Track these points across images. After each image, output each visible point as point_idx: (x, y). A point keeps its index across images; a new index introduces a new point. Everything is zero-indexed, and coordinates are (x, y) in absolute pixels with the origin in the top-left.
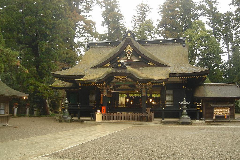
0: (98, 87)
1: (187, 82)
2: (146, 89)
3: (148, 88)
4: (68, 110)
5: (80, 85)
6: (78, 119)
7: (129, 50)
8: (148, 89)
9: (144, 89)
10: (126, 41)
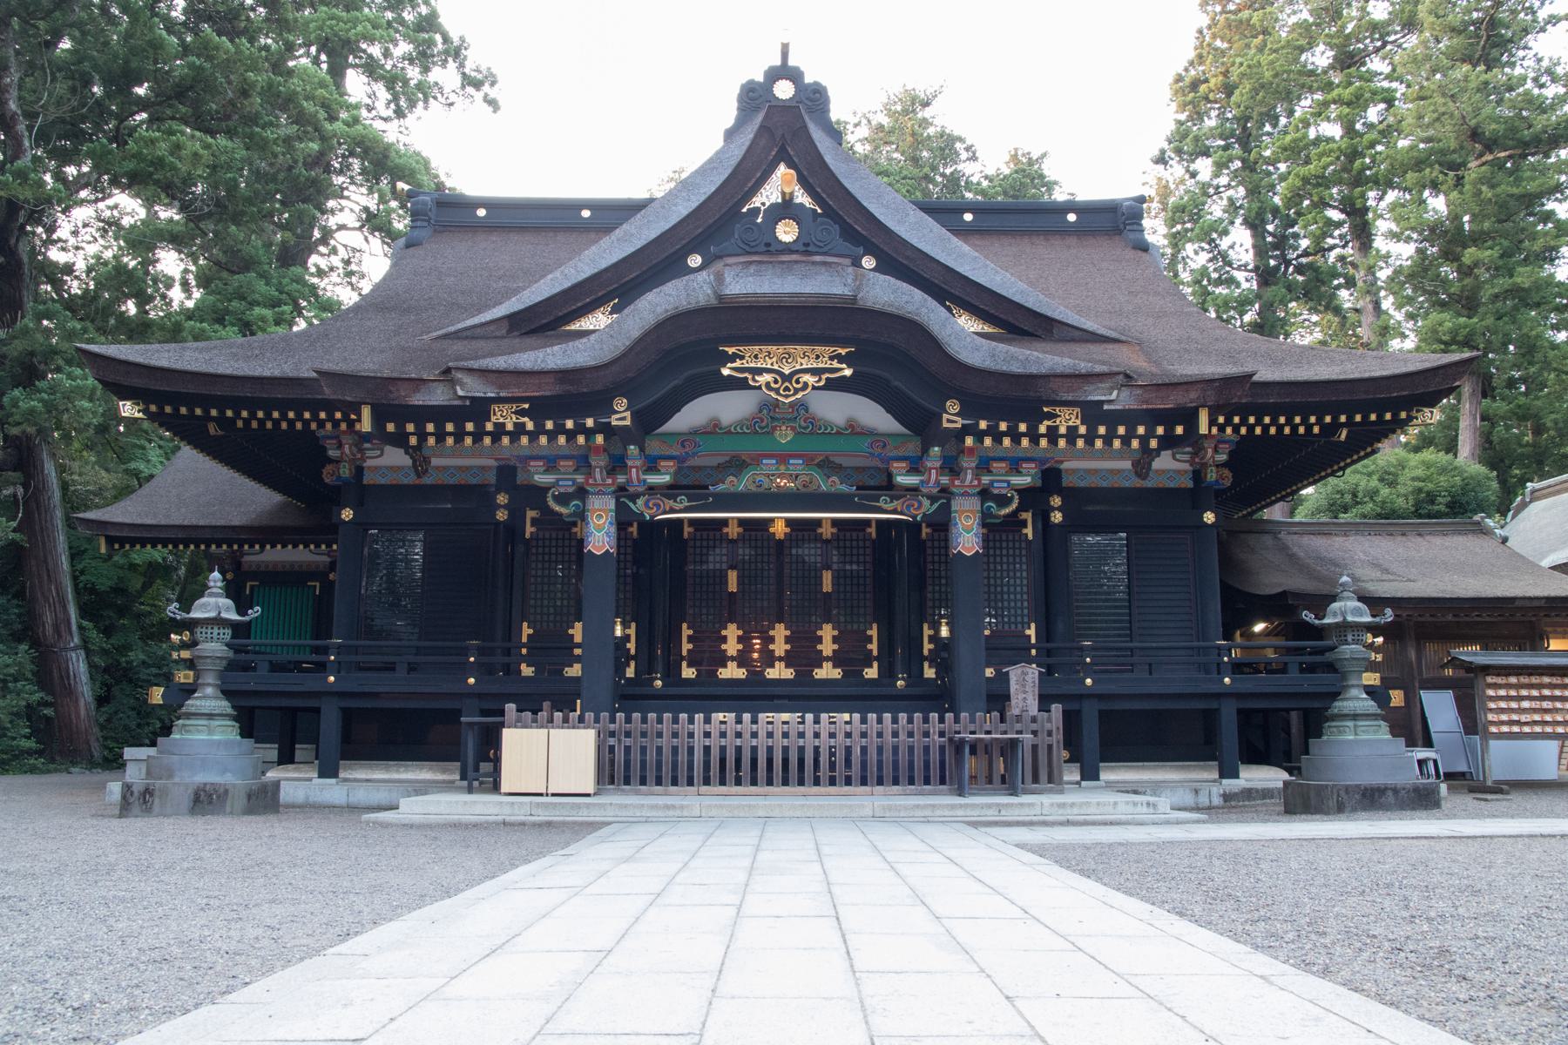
0: (536, 477)
2: (985, 494)
6: (321, 776)
8: (1003, 501)
9: (965, 494)
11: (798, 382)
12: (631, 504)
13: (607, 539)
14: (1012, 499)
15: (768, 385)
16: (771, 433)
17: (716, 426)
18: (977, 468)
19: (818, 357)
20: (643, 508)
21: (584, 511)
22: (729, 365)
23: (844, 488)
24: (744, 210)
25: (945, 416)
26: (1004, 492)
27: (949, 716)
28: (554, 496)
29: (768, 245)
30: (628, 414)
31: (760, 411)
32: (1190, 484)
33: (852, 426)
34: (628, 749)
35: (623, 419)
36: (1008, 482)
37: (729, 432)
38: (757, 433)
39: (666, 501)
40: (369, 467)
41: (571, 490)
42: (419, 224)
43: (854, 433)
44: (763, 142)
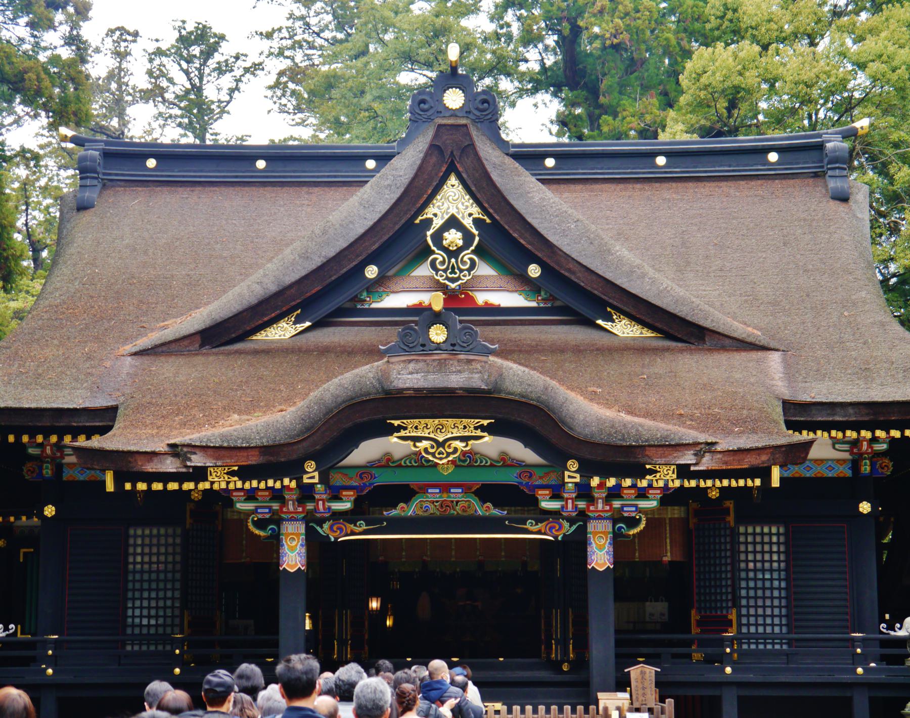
1: (887, 467)
2: (617, 518)
3: (629, 512)
5: (110, 487)
7: (453, 223)
8: (632, 522)
9: (599, 518)
10: (434, 148)
11: (449, 446)
12: (318, 529)
13: (299, 559)
14: (640, 518)
15: (426, 450)
17: (388, 460)
18: (606, 497)
19: (465, 427)
20: (328, 532)
21: (279, 534)
22: (396, 434)
23: (496, 512)
24: (417, 221)
25: (567, 473)
26: (633, 515)
27: (580, 708)
28: (253, 521)
29: (423, 345)
30: (316, 474)
32: (849, 474)
33: (503, 459)
35: (313, 477)
36: (636, 506)
37: (400, 466)
38: (423, 466)
39: (348, 525)
40: (66, 464)
41: (268, 516)
42: (88, 182)
43: (505, 465)
44: (434, 159)
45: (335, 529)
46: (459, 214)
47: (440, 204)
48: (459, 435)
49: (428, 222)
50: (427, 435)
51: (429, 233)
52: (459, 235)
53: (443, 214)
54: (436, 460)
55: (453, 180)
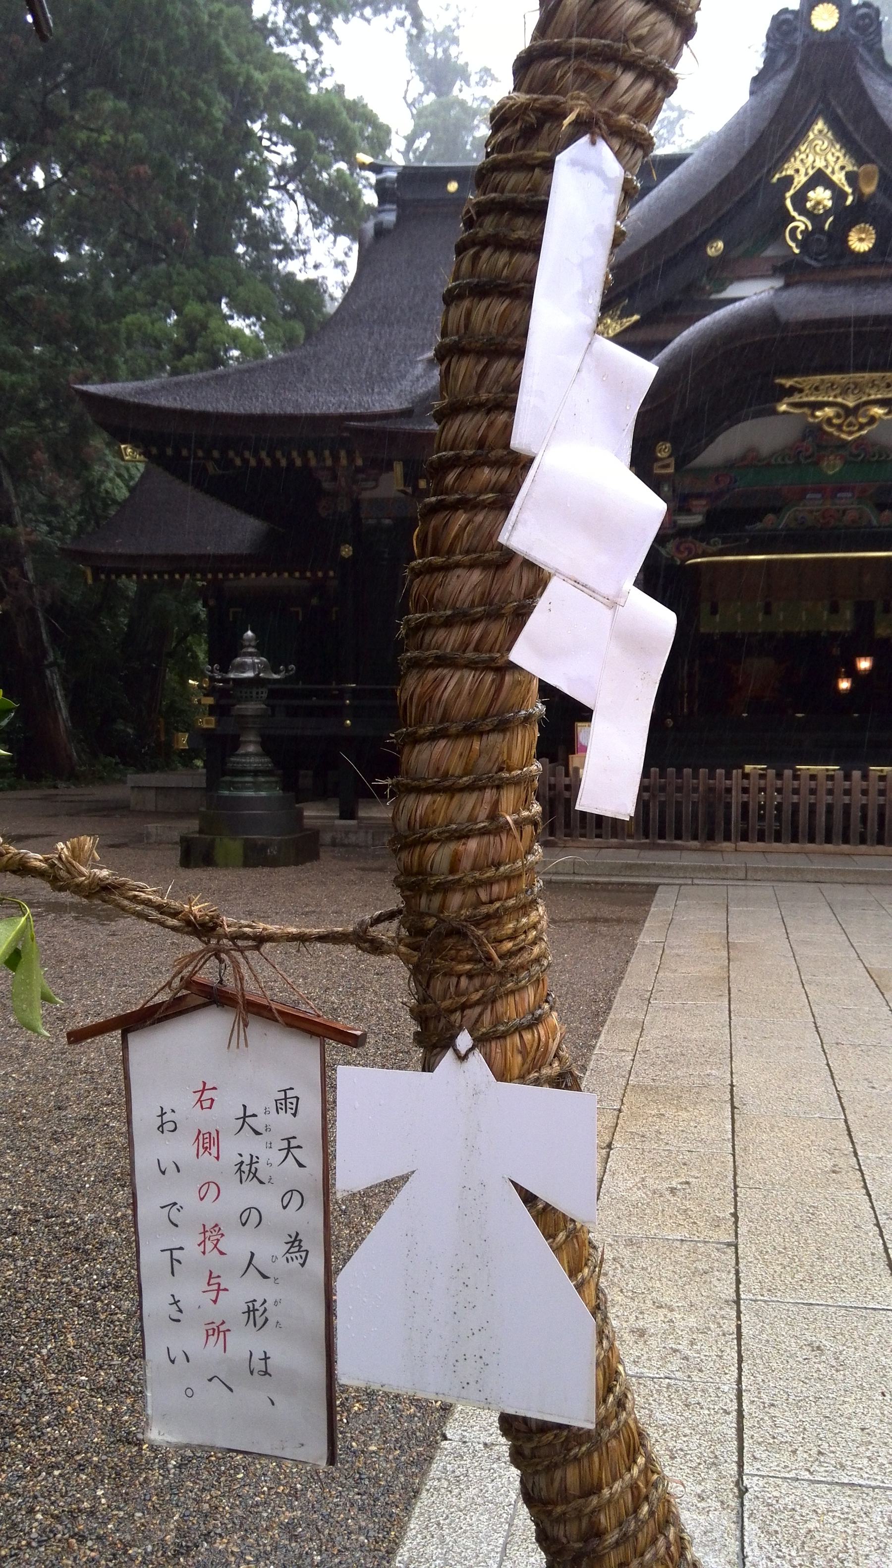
4: (268, 745)
6: (342, 817)
7: (819, 178)
16: (817, 463)
22: (786, 400)
24: (775, 180)
30: (672, 461)
31: (804, 438)
34: (662, 805)
37: (768, 465)
39: (698, 543)
45: (682, 548)
46: (827, 167)
47: (803, 156)
48: (879, 396)
49: (789, 180)
50: (831, 399)
51: (788, 195)
52: (828, 194)
53: (807, 169)
54: (844, 436)
55: (820, 125)
